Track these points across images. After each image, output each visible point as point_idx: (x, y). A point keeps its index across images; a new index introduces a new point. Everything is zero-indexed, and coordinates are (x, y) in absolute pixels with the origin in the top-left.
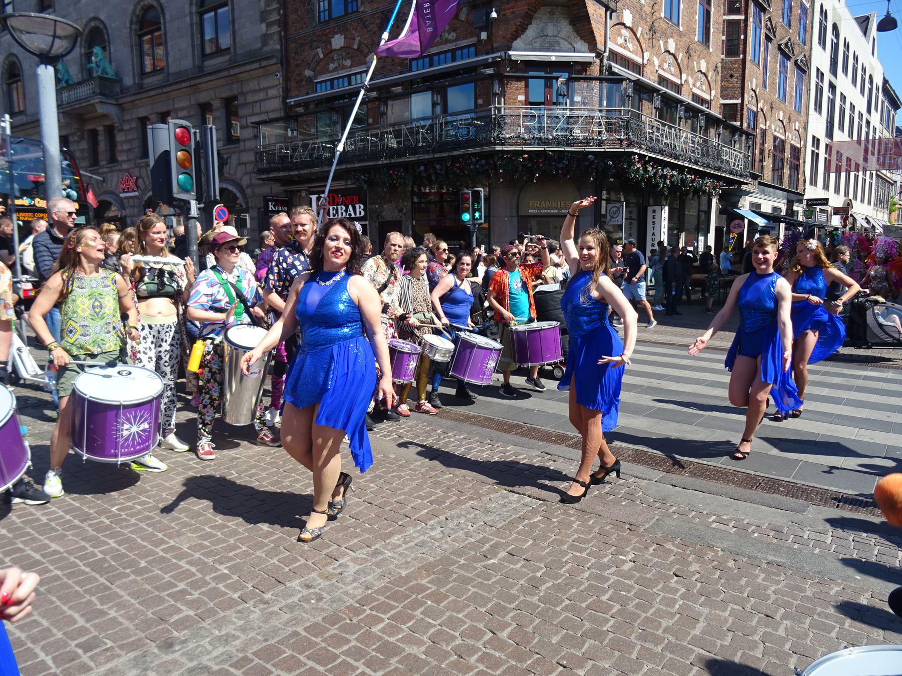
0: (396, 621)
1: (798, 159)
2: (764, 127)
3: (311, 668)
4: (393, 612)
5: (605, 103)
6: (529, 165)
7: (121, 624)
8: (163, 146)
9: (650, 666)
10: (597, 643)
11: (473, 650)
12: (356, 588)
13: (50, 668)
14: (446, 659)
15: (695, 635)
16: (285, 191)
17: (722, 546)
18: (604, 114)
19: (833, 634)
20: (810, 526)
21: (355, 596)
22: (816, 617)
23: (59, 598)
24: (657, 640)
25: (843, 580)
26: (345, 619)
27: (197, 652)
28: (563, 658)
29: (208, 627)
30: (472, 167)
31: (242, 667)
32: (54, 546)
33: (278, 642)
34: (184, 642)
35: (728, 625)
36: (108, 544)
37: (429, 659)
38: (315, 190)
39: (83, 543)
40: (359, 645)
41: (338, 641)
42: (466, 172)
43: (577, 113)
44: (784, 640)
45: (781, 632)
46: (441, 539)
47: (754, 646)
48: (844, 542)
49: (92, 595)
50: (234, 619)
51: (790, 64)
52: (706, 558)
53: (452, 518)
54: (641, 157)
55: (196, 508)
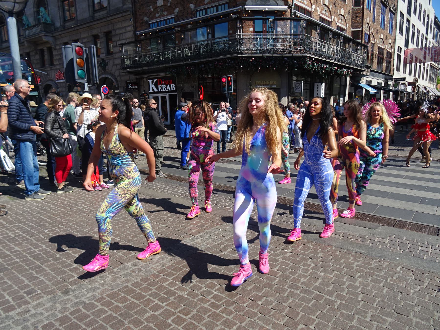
0: (175, 280)
1: (390, 58)
2: (373, 42)
3: (133, 302)
4: (174, 277)
5: (293, 32)
6: (255, 63)
7: (45, 283)
8: (70, 57)
9: (293, 299)
10: (269, 289)
11: (209, 293)
12: (157, 266)
13: (11, 303)
14: (196, 297)
15: (316, 285)
16: (136, 78)
17: (335, 245)
19: (382, 285)
20: (379, 235)
21: (157, 269)
22: (374, 277)
23: (17, 272)
24: (297, 288)
25: (390, 260)
26: (151, 280)
27: (80, 295)
28: (252, 296)
29: (86, 284)
30: (227, 65)
31: (100, 301)
32: (16, 248)
33: (118, 290)
34: (74, 291)
35: (332, 281)
36: (42, 247)
37: (189, 297)
38: (151, 77)
39: (30, 247)
40: (156, 291)
41: (146, 290)
43: (278, 36)
44: (357, 287)
45: (357, 284)
46: (201, 243)
47: (343, 290)
48: (393, 243)
49: (33, 270)
50: (98, 280)
51: (387, 10)
52: (326, 251)
53: (207, 233)
55: (85, 230)
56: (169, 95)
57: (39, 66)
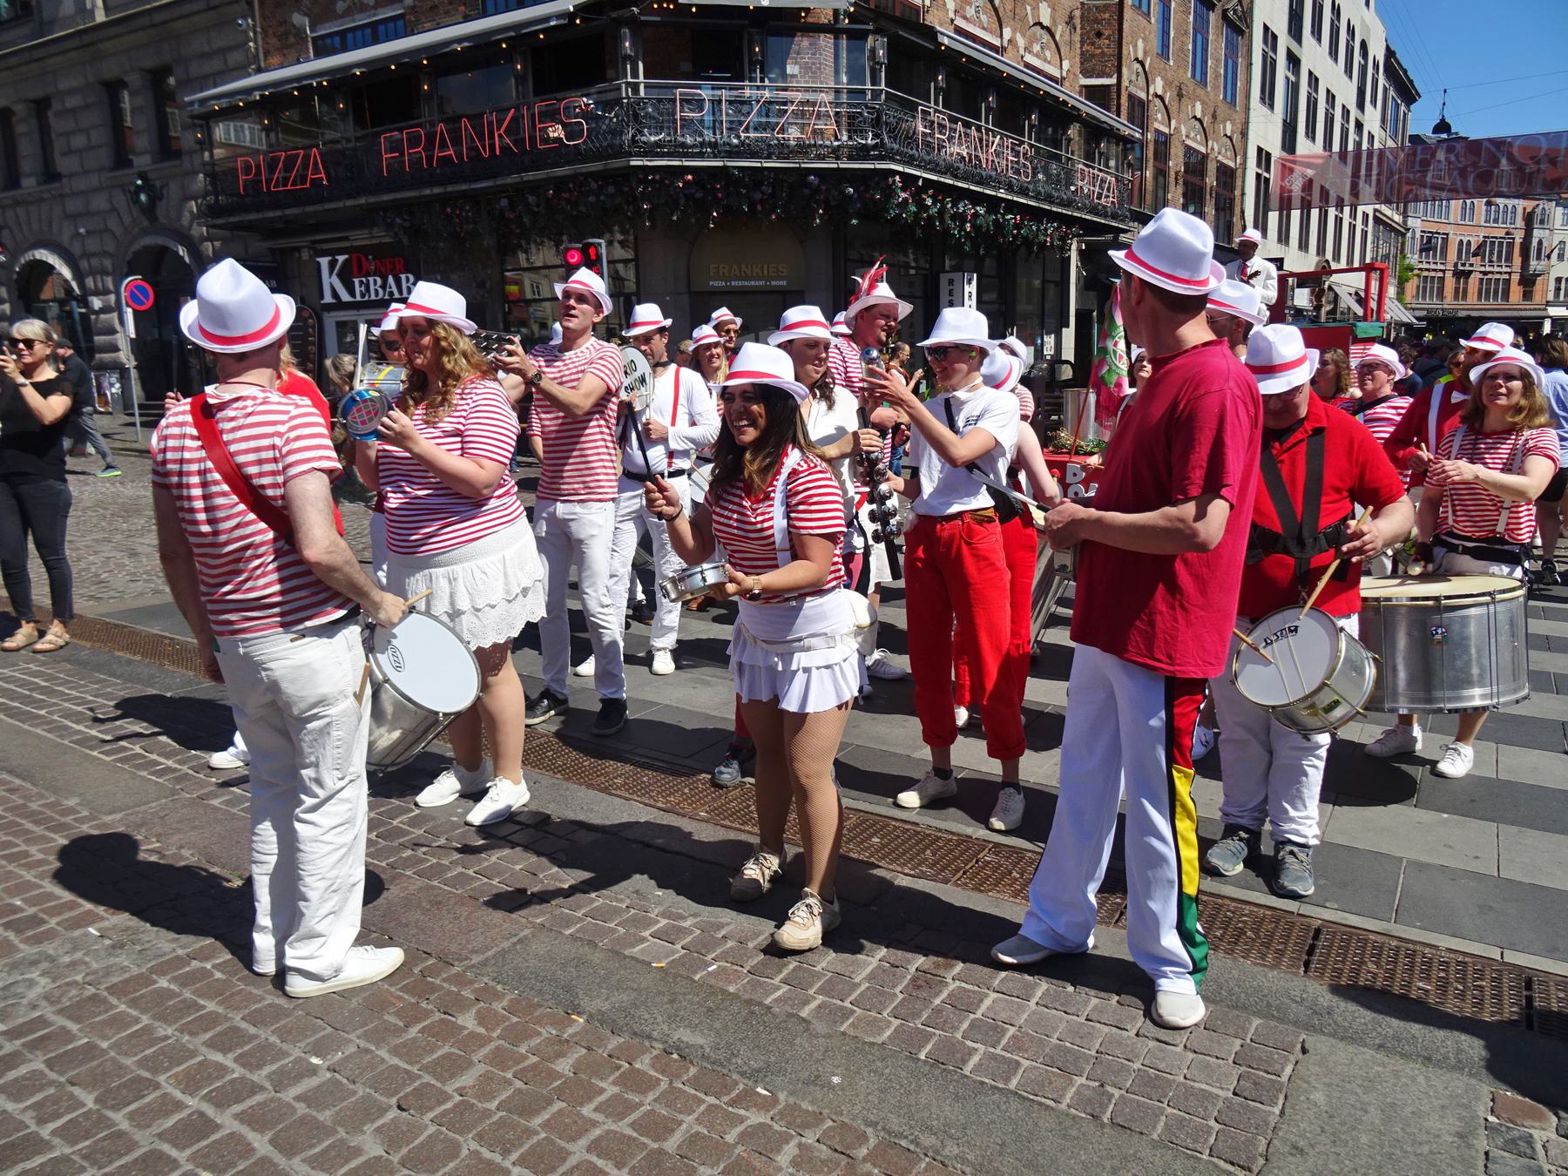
1: (1232, 189)
2: (1166, 130)
5: (845, 79)
6: (699, 195)
18: (844, 98)
30: (592, 199)
42: (582, 209)
51: (1214, 18)
54: (909, 180)
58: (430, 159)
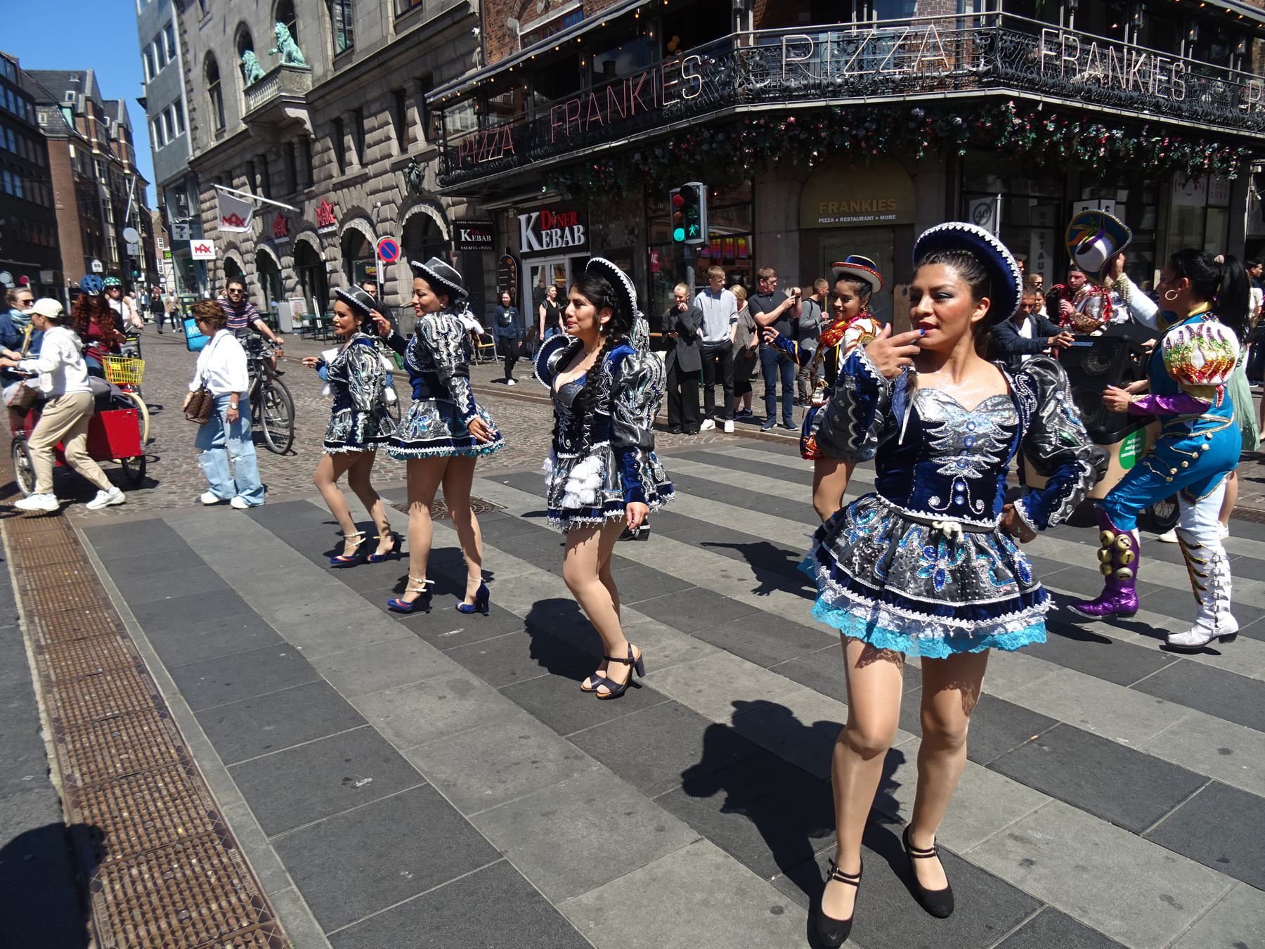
6: (802, 136)
30: (705, 147)
38: (526, 205)
54: (1024, 107)
56: (573, 261)
57: (284, 191)
58: (584, 124)
